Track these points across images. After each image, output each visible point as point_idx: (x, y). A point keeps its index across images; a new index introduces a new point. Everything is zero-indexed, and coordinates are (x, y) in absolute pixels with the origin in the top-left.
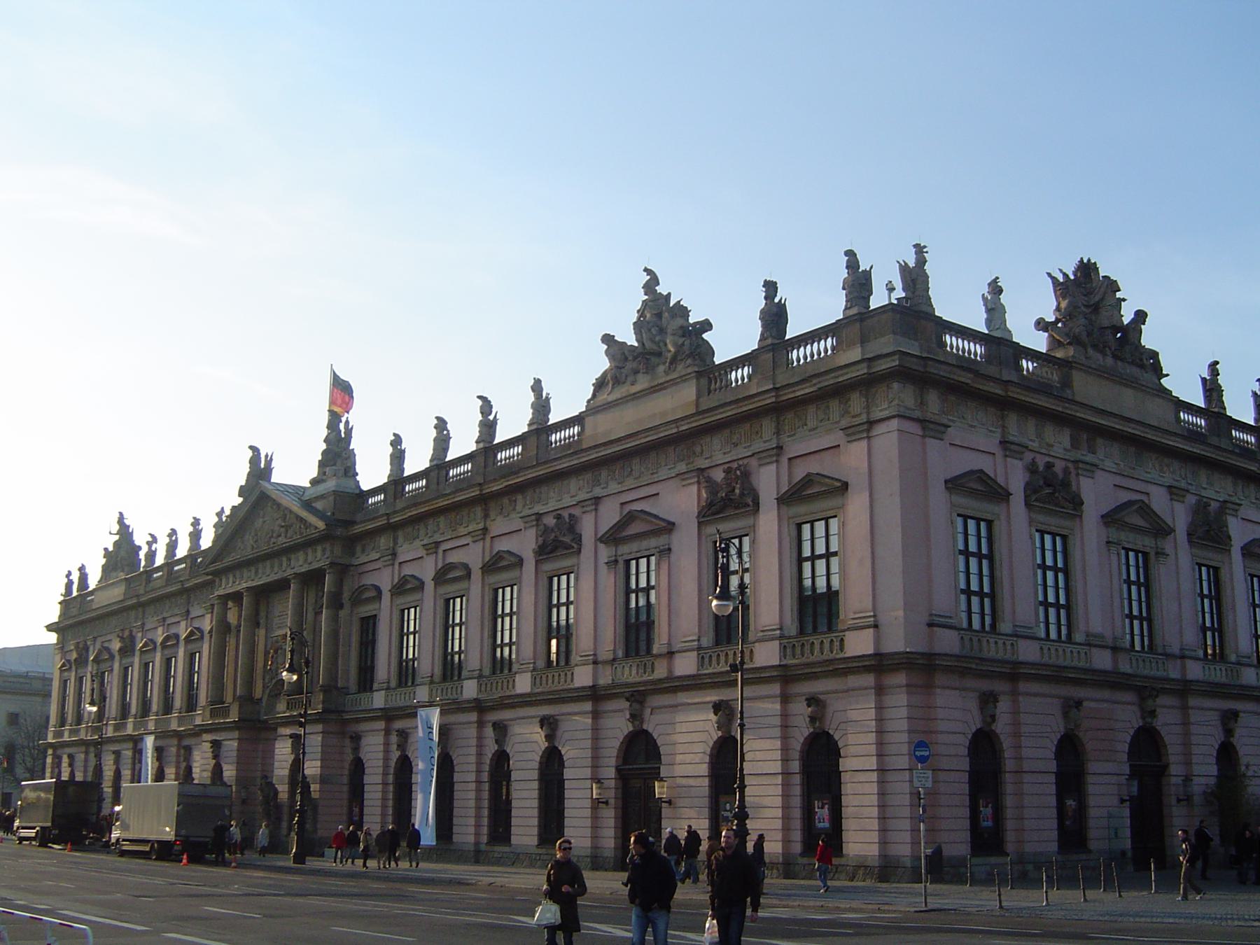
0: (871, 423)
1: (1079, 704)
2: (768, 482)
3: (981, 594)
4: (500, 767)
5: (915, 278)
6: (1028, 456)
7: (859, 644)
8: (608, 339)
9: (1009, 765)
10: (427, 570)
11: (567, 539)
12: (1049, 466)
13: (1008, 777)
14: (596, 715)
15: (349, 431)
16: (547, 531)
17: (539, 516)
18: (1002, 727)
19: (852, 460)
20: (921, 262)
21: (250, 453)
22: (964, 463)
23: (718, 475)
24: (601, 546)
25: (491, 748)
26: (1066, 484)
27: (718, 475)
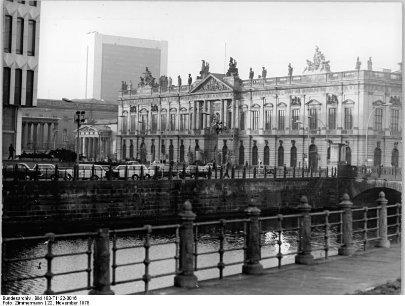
0: (359, 92)
1: (398, 143)
2: (340, 98)
3: (379, 123)
4: (281, 150)
5: (370, 63)
6: (390, 96)
7: (355, 132)
8: (308, 61)
9: (382, 154)
10: (261, 103)
11: (297, 103)
12: (395, 97)
13: (382, 157)
14: (304, 140)
15: (236, 63)
16: (293, 100)
17: (291, 96)
18: (381, 148)
19: (354, 98)
20: (370, 60)
21: (202, 62)
22: (376, 99)
23: (331, 96)
24: (306, 106)
25: (278, 145)
26: (399, 100)
27: (331, 96)
